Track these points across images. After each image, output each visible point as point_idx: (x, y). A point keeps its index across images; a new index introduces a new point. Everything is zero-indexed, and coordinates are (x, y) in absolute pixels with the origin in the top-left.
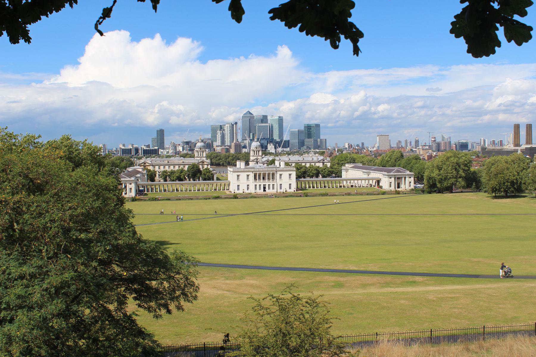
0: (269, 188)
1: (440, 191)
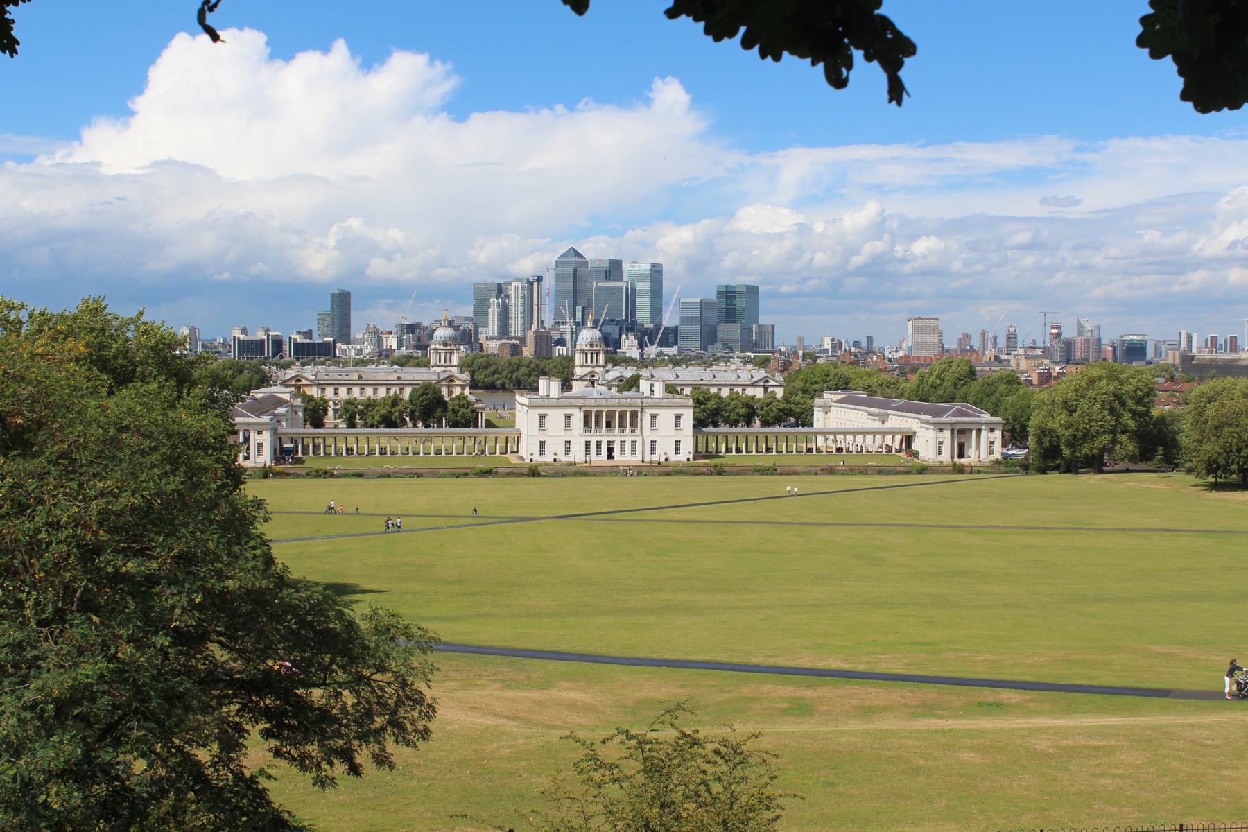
0: (623, 451)
1: (1071, 467)
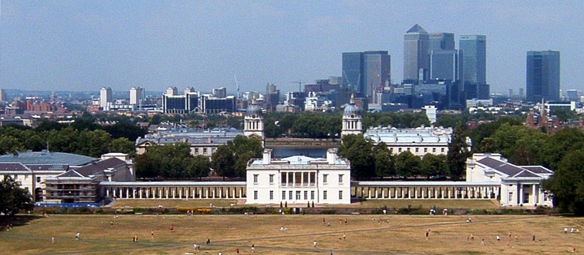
0: (306, 198)
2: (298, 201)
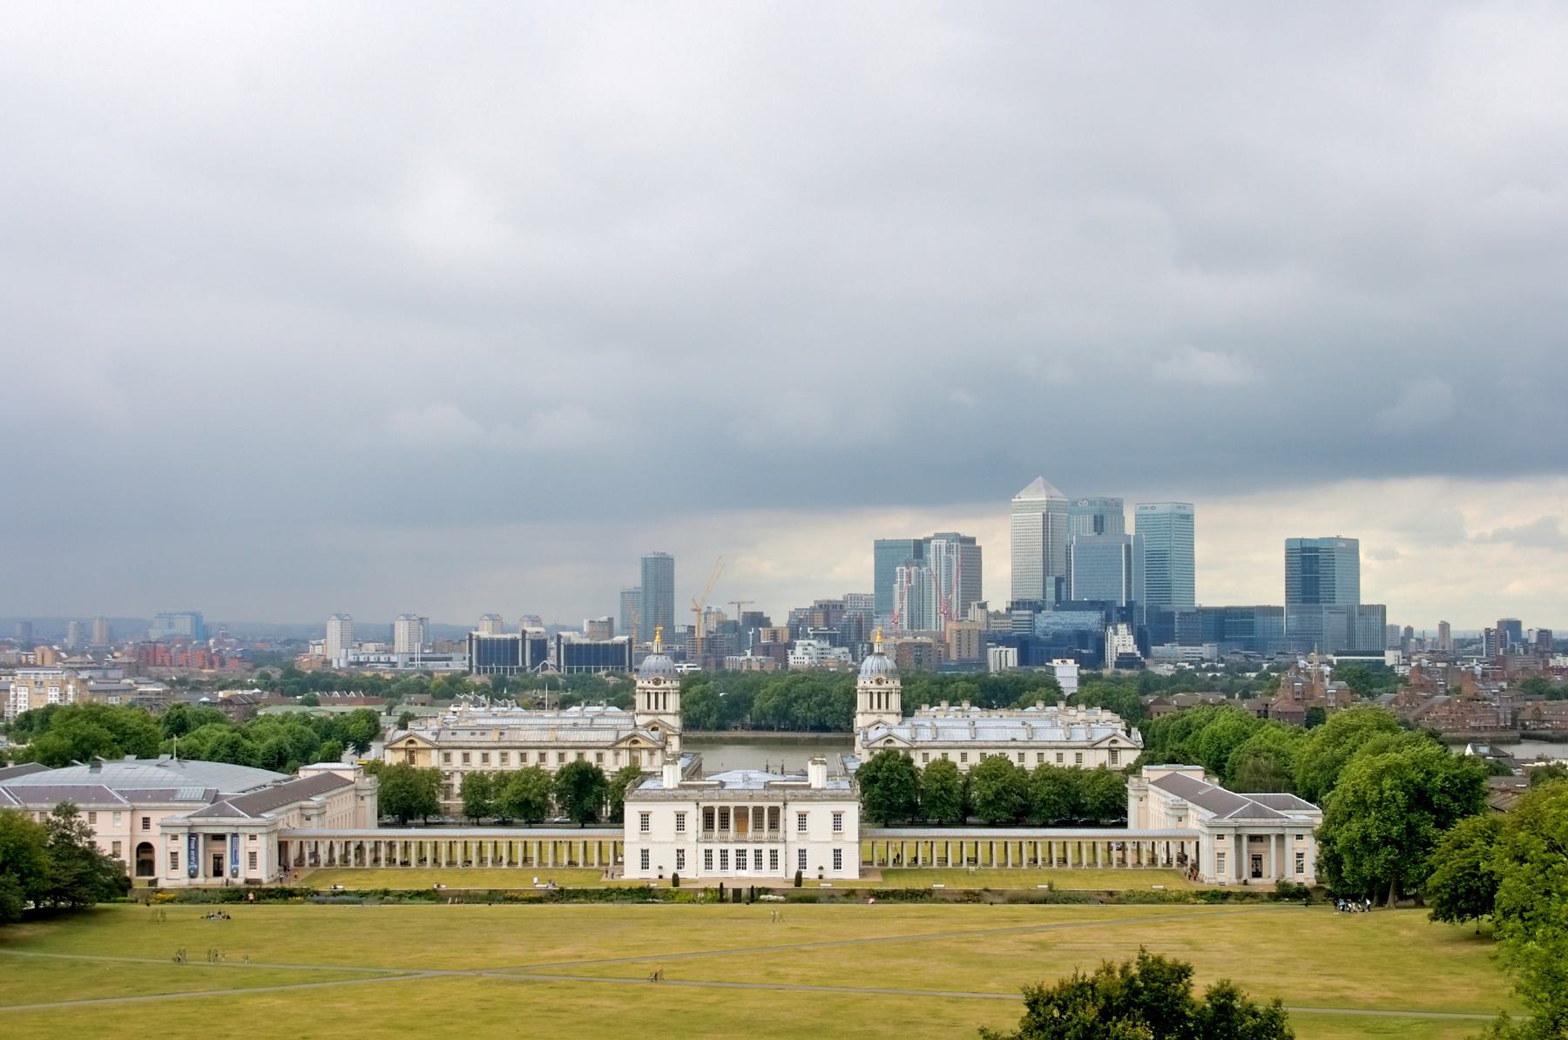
2: (741, 873)
